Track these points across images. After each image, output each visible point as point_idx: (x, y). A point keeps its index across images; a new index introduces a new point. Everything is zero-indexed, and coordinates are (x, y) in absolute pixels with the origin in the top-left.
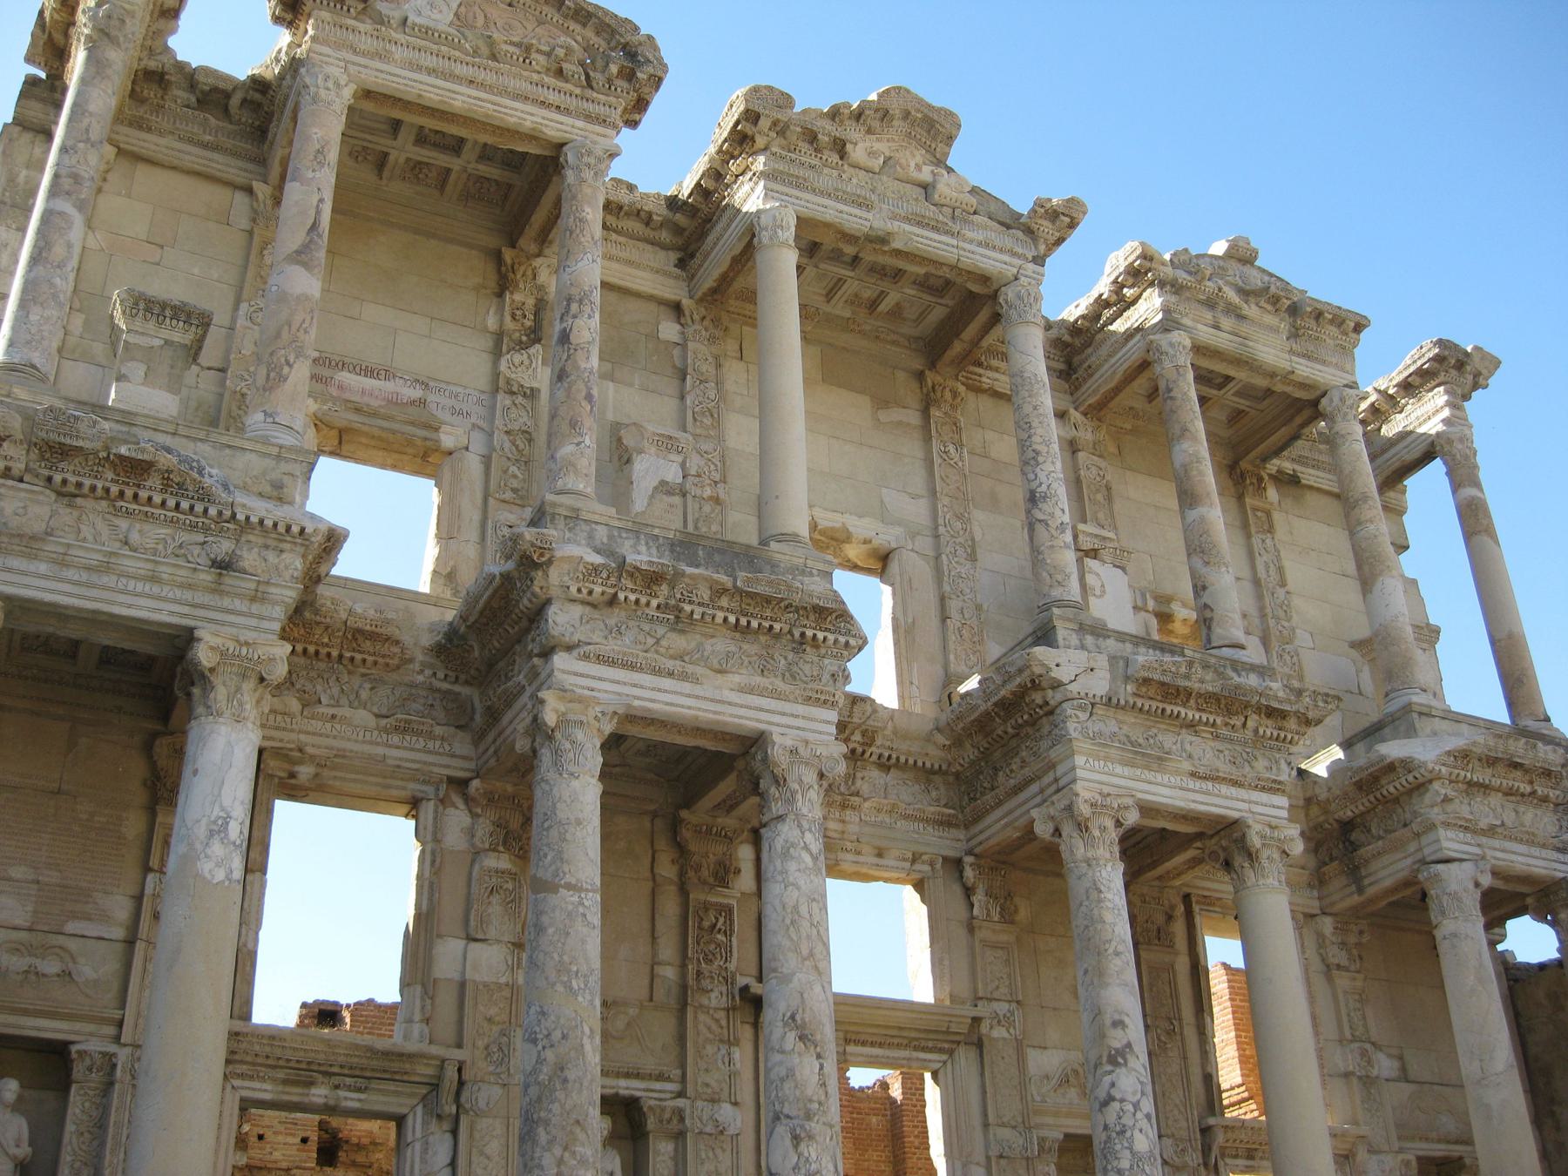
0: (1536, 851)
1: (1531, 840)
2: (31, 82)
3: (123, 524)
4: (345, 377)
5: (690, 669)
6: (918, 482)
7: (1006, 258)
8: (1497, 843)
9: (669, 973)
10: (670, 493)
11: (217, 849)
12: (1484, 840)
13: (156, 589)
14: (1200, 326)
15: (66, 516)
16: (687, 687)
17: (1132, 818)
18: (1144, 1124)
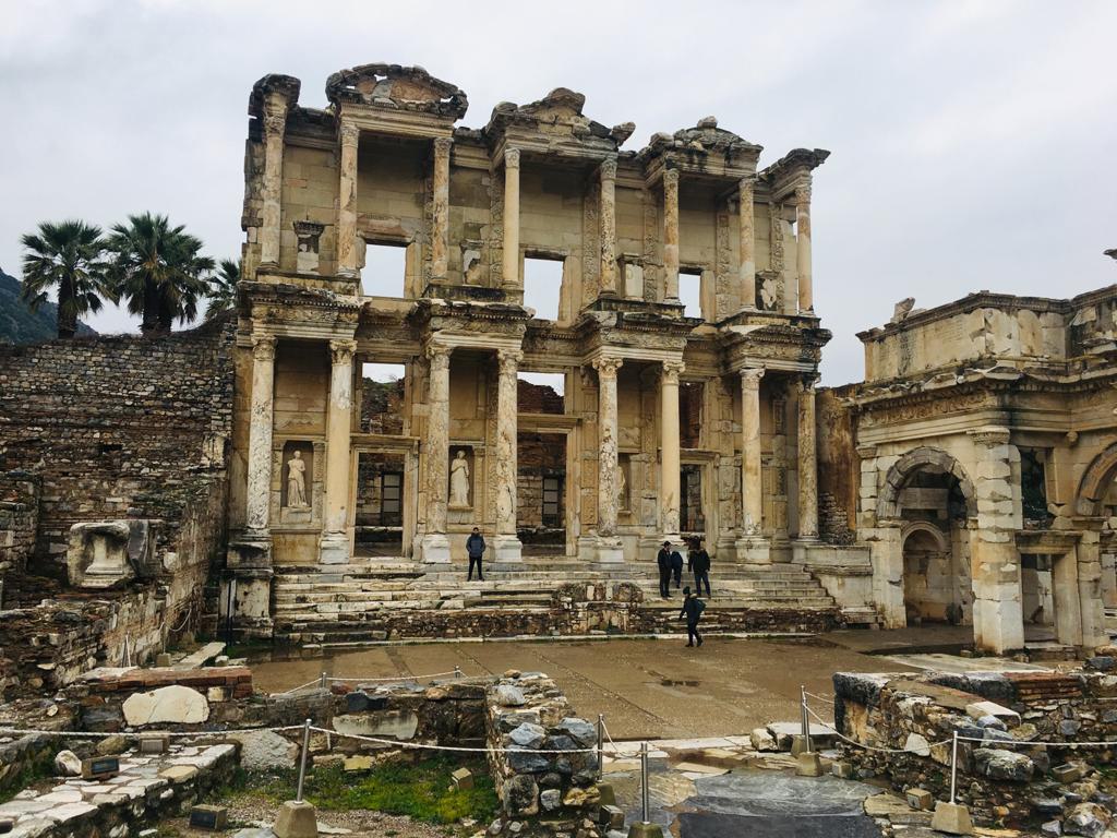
2: (252, 122)
4: (373, 221)
6: (578, 229)
9: (482, 409)
13: (316, 329)
16: (473, 338)
17: (620, 365)
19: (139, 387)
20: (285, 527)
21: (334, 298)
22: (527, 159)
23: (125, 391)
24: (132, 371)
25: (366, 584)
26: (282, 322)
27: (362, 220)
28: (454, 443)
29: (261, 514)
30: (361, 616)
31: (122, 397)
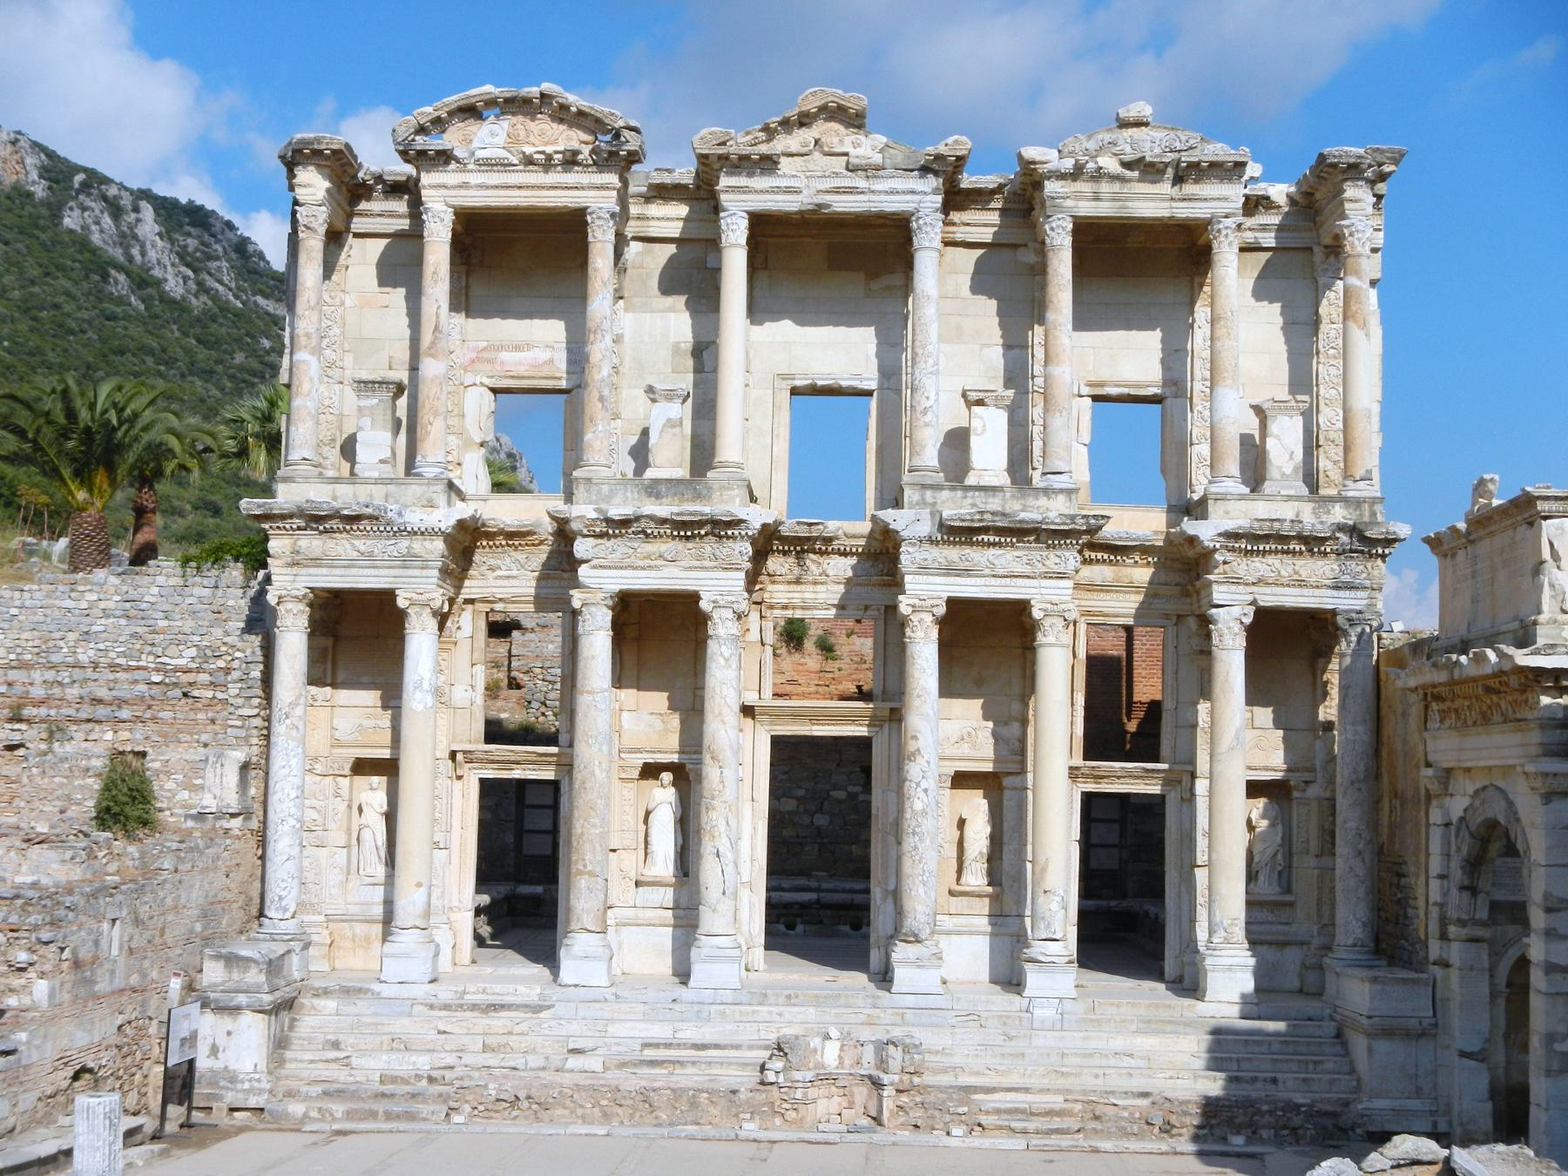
0: (1309, 592)
1: (1301, 583)
3: (356, 542)
4: (505, 356)
5: (653, 563)
7: (909, 197)
8: (1268, 590)
10: (673, 426)
11: (418, 695)
12: (1255, 589)
13: (375, 572)
14: (1081, 204)
15: (330, 543)
16: (653, 573)
17: (941, 610)
18: (922, 795)
19: (173, 650)
20: (354, 909)
21: (400, 514)
22: (761, 224)
23: (151, 658)
24: (162, 623)
25: (443, 1020)
26: (316, 561)
27: (485, 355)
28: (651, 758)
29: (283, 893)
30: (418, 1077)
31: (145, 668)
